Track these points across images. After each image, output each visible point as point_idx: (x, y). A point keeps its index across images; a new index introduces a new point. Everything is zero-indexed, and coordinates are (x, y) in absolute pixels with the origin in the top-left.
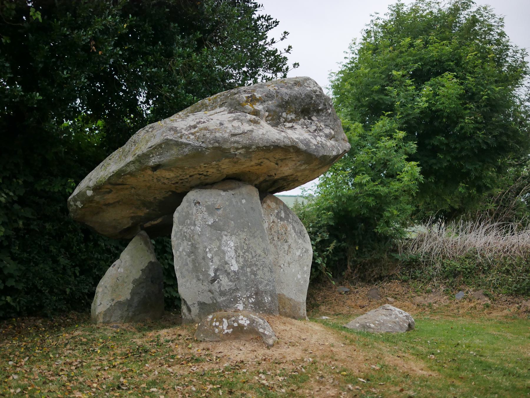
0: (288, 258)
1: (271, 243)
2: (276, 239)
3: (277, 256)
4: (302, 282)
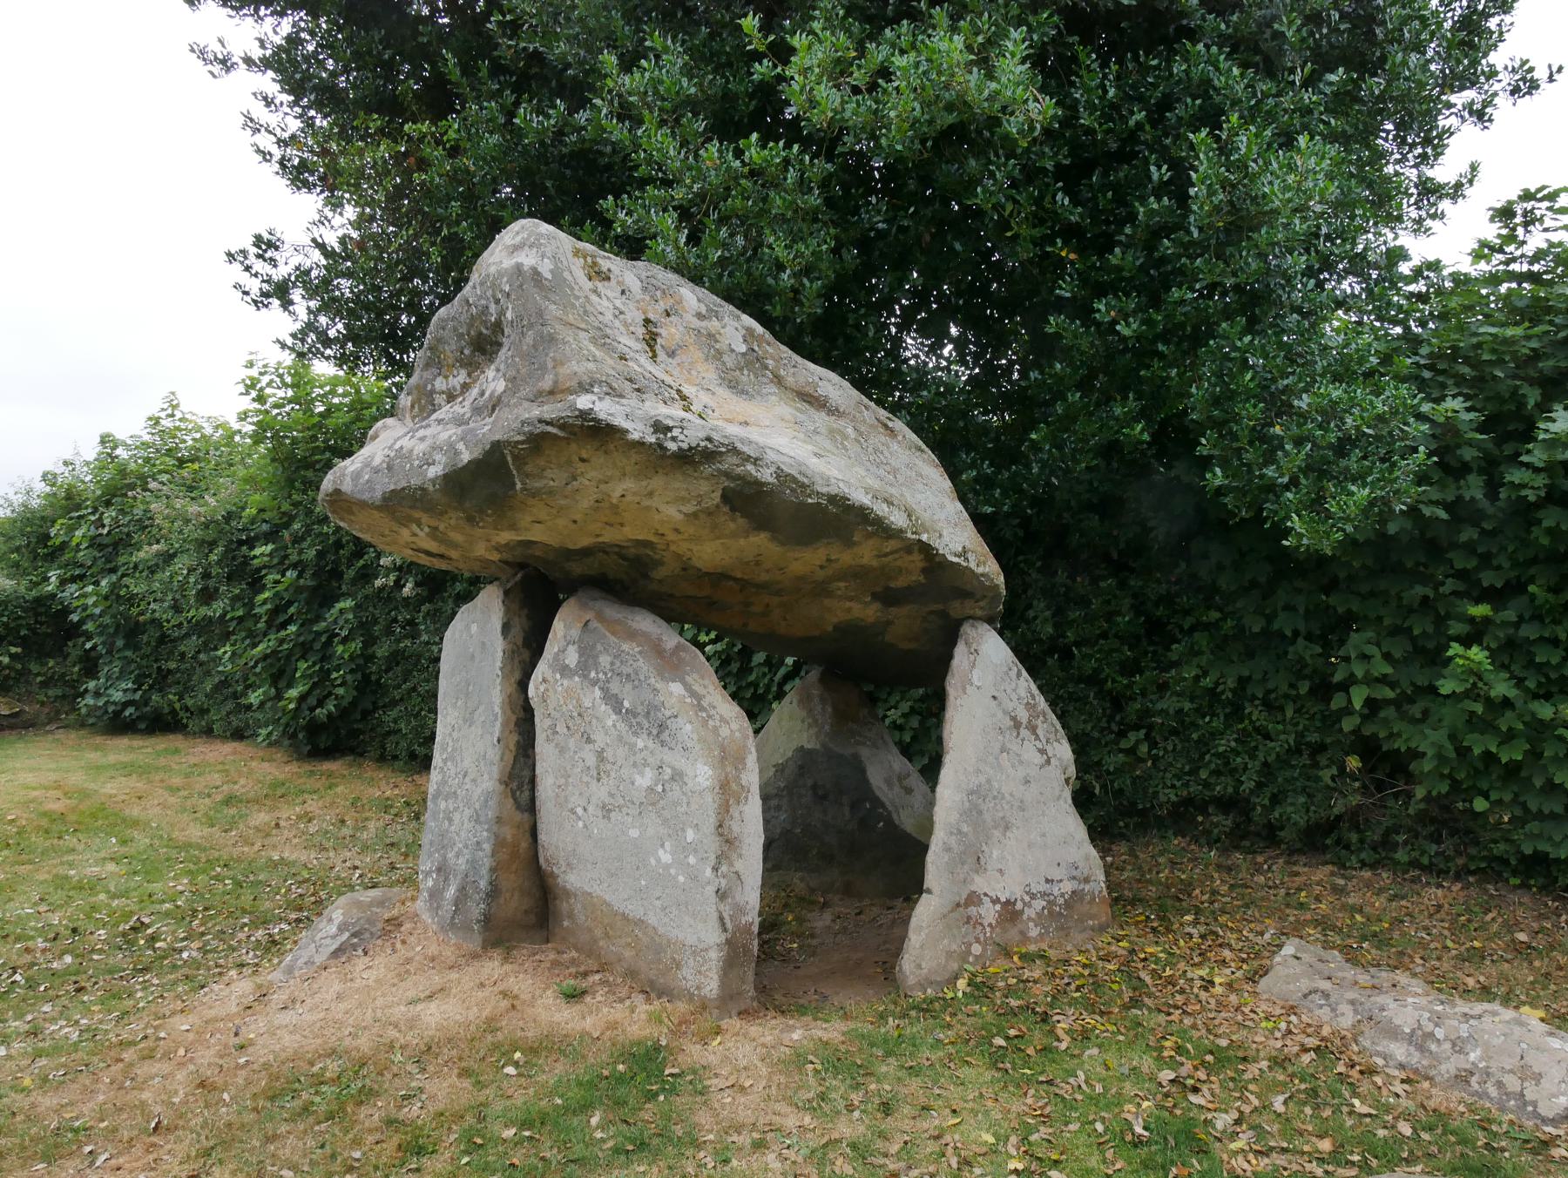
0: (600, 792)
2: (561, 728)
4: (681, 879)
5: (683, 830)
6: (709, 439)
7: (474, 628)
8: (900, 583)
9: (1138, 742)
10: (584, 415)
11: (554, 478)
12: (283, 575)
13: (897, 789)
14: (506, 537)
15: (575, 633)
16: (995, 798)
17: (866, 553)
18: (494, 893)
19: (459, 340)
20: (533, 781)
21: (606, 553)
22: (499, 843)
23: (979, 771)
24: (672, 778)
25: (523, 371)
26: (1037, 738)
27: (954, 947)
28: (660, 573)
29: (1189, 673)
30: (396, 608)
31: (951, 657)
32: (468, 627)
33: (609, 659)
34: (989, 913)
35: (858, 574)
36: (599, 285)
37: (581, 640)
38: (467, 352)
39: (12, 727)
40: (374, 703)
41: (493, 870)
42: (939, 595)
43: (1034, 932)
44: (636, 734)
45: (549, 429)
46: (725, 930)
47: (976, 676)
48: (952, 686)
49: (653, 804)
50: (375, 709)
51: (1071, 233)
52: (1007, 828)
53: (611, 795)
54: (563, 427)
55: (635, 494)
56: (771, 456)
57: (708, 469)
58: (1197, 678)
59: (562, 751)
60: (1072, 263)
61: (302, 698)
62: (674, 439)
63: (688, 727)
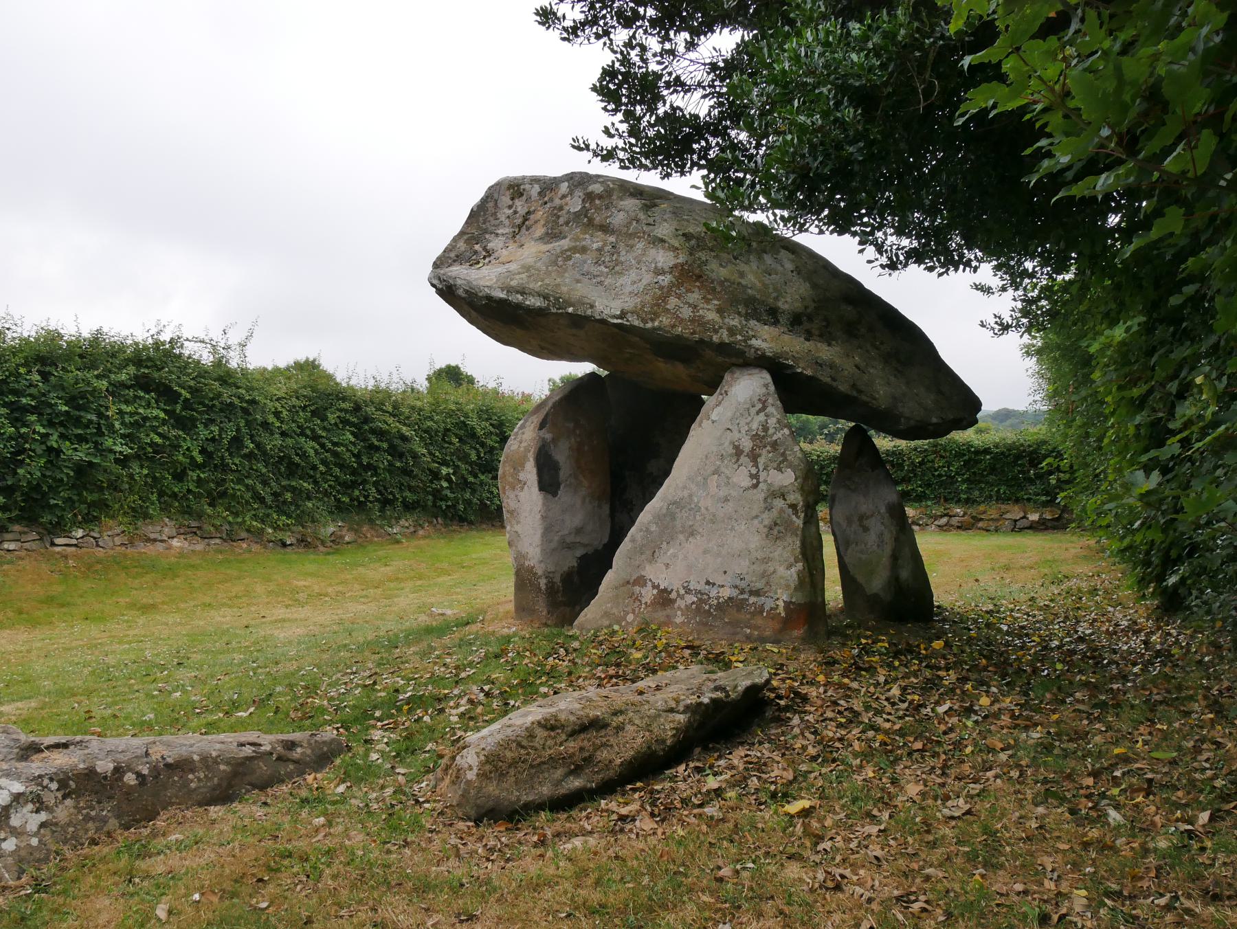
13: (855, 526)
27: (615, 611)
34: (648, 594)
39: (1054, 528)
43: (679, 619)
52: (692, 534)
56: (459, 282)
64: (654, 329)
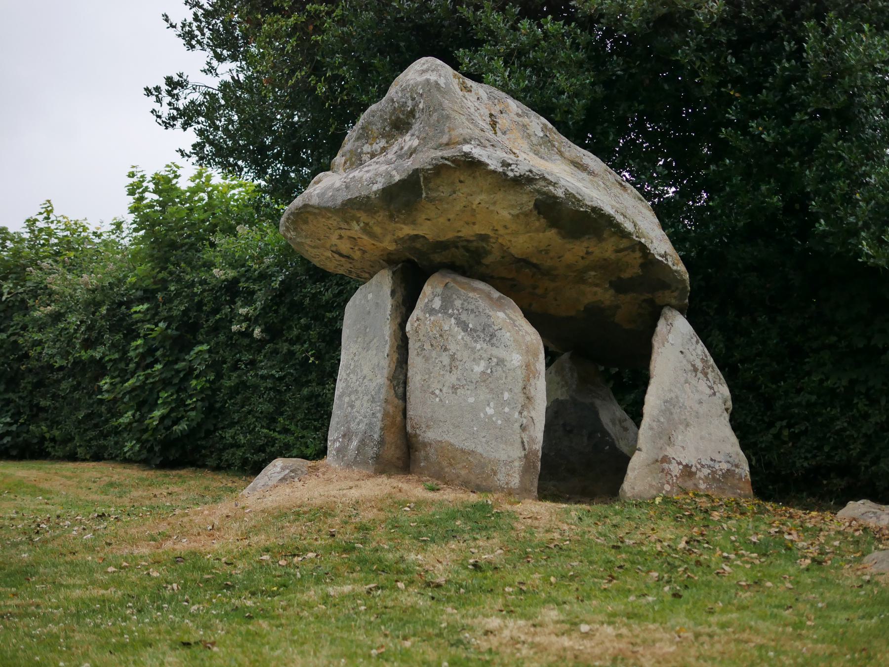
0: (452, 379)
1: (418, 355)
2: (427, 346)
3: (427, 376)
4: (499, 422)
5: (502, 393)
6: (531, 171)
7: (370, 296)
8: (626, 275)
9: (781, 428)
10: (466, 155)
11: (444, 191)
12: (157, 326)
13: (618, 427)
14: (407, 230)
15: (439, 290)
16: (680, 407)
17: (606, 249)
18: (382, 442)
19: (383, 123)
20: (405, 383)
21: (457, 247)
22: (386, 415)
23: (671, 390)
24: (497, 364)
25: (430, 134)
26: (708, 379)
28: (488, 260)
29: (815, 378)
30: (240, 352)
31: (656, 326)
32: (366, 297)
33: (460, 302)
34: (676, 470)
35: (604, 266)
36: (466, 94)
37: (443, 294)
38: (387, 129)
40: (215, 425)
41: (382, 429)
42: (647, 290)
44: (476, 341)
45: (447, 162)
46: (525, 449)
47: (671, 337)
48: (656, 342)
49: (484, 381)
50: (216, 430)
51: (737, 81)
52: (687, 425)
53: (458, 379)
54: (453, 161)
55: (486, 202)
56: (562, 182)
57: (529, 188)
58: (821, 381)
59: (427, 359)
60: (737, 99)
61: (162, 418)
62: (512, 170)
63: (508, 334)
64: (676, 271)
